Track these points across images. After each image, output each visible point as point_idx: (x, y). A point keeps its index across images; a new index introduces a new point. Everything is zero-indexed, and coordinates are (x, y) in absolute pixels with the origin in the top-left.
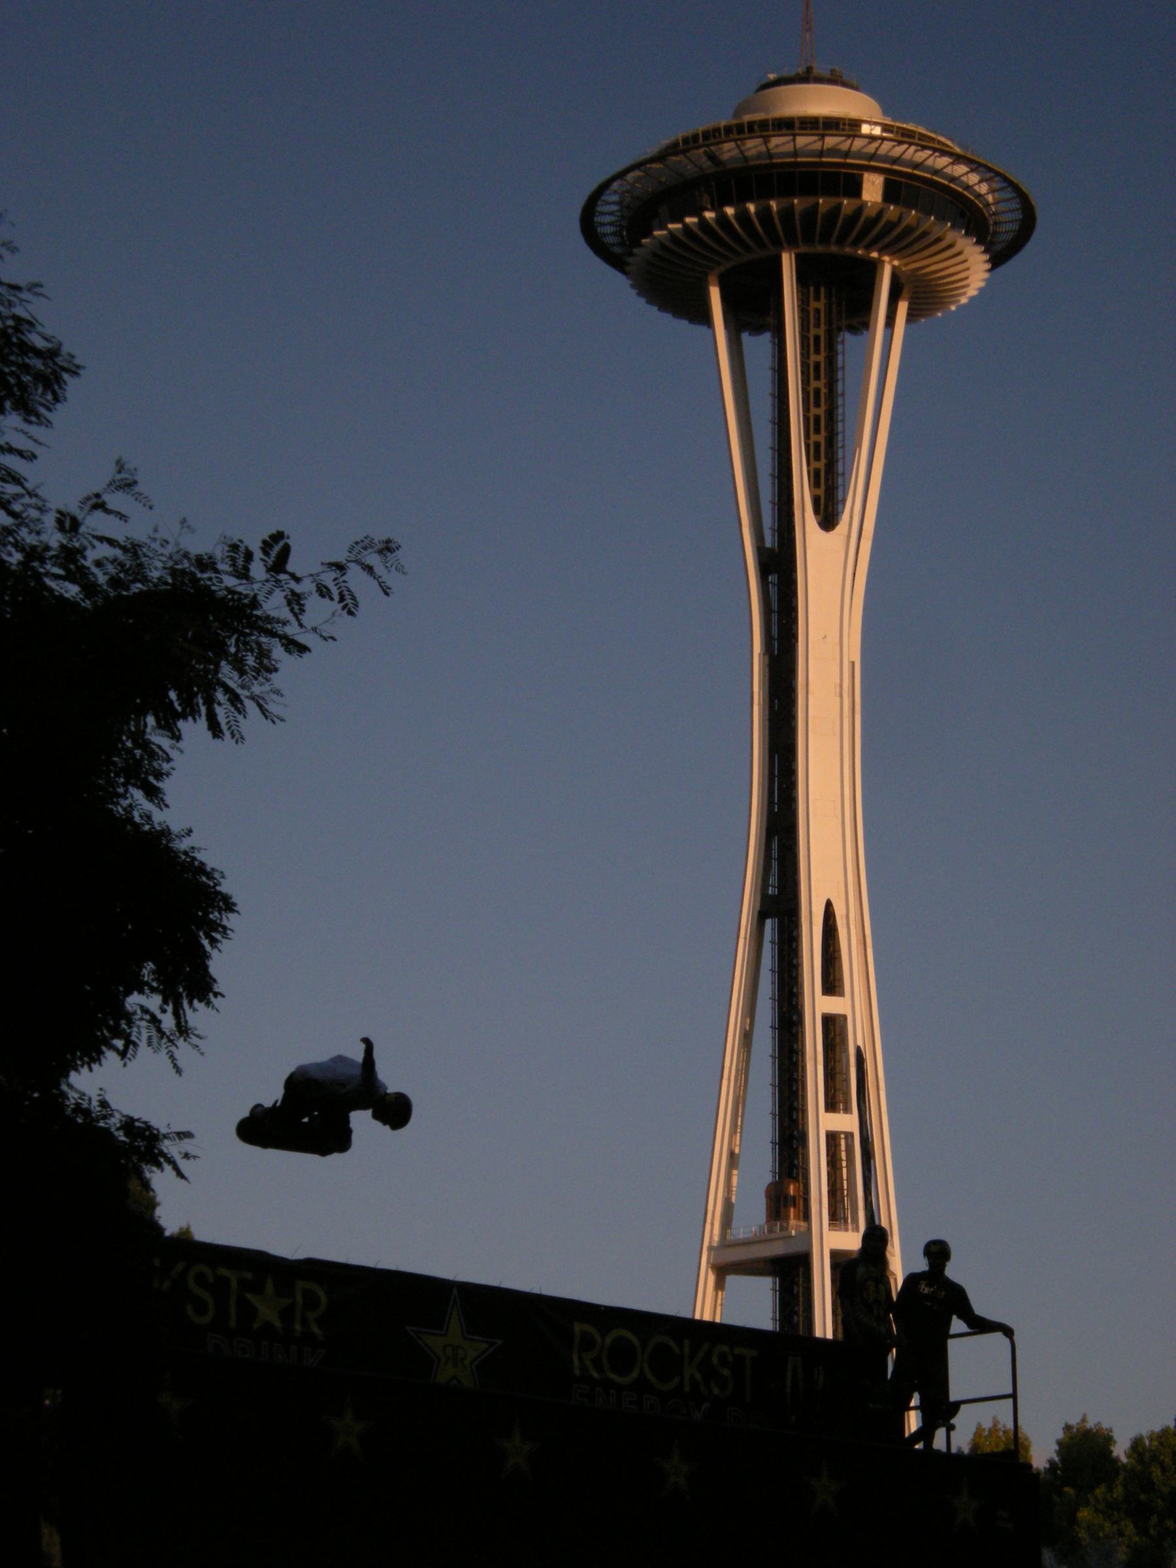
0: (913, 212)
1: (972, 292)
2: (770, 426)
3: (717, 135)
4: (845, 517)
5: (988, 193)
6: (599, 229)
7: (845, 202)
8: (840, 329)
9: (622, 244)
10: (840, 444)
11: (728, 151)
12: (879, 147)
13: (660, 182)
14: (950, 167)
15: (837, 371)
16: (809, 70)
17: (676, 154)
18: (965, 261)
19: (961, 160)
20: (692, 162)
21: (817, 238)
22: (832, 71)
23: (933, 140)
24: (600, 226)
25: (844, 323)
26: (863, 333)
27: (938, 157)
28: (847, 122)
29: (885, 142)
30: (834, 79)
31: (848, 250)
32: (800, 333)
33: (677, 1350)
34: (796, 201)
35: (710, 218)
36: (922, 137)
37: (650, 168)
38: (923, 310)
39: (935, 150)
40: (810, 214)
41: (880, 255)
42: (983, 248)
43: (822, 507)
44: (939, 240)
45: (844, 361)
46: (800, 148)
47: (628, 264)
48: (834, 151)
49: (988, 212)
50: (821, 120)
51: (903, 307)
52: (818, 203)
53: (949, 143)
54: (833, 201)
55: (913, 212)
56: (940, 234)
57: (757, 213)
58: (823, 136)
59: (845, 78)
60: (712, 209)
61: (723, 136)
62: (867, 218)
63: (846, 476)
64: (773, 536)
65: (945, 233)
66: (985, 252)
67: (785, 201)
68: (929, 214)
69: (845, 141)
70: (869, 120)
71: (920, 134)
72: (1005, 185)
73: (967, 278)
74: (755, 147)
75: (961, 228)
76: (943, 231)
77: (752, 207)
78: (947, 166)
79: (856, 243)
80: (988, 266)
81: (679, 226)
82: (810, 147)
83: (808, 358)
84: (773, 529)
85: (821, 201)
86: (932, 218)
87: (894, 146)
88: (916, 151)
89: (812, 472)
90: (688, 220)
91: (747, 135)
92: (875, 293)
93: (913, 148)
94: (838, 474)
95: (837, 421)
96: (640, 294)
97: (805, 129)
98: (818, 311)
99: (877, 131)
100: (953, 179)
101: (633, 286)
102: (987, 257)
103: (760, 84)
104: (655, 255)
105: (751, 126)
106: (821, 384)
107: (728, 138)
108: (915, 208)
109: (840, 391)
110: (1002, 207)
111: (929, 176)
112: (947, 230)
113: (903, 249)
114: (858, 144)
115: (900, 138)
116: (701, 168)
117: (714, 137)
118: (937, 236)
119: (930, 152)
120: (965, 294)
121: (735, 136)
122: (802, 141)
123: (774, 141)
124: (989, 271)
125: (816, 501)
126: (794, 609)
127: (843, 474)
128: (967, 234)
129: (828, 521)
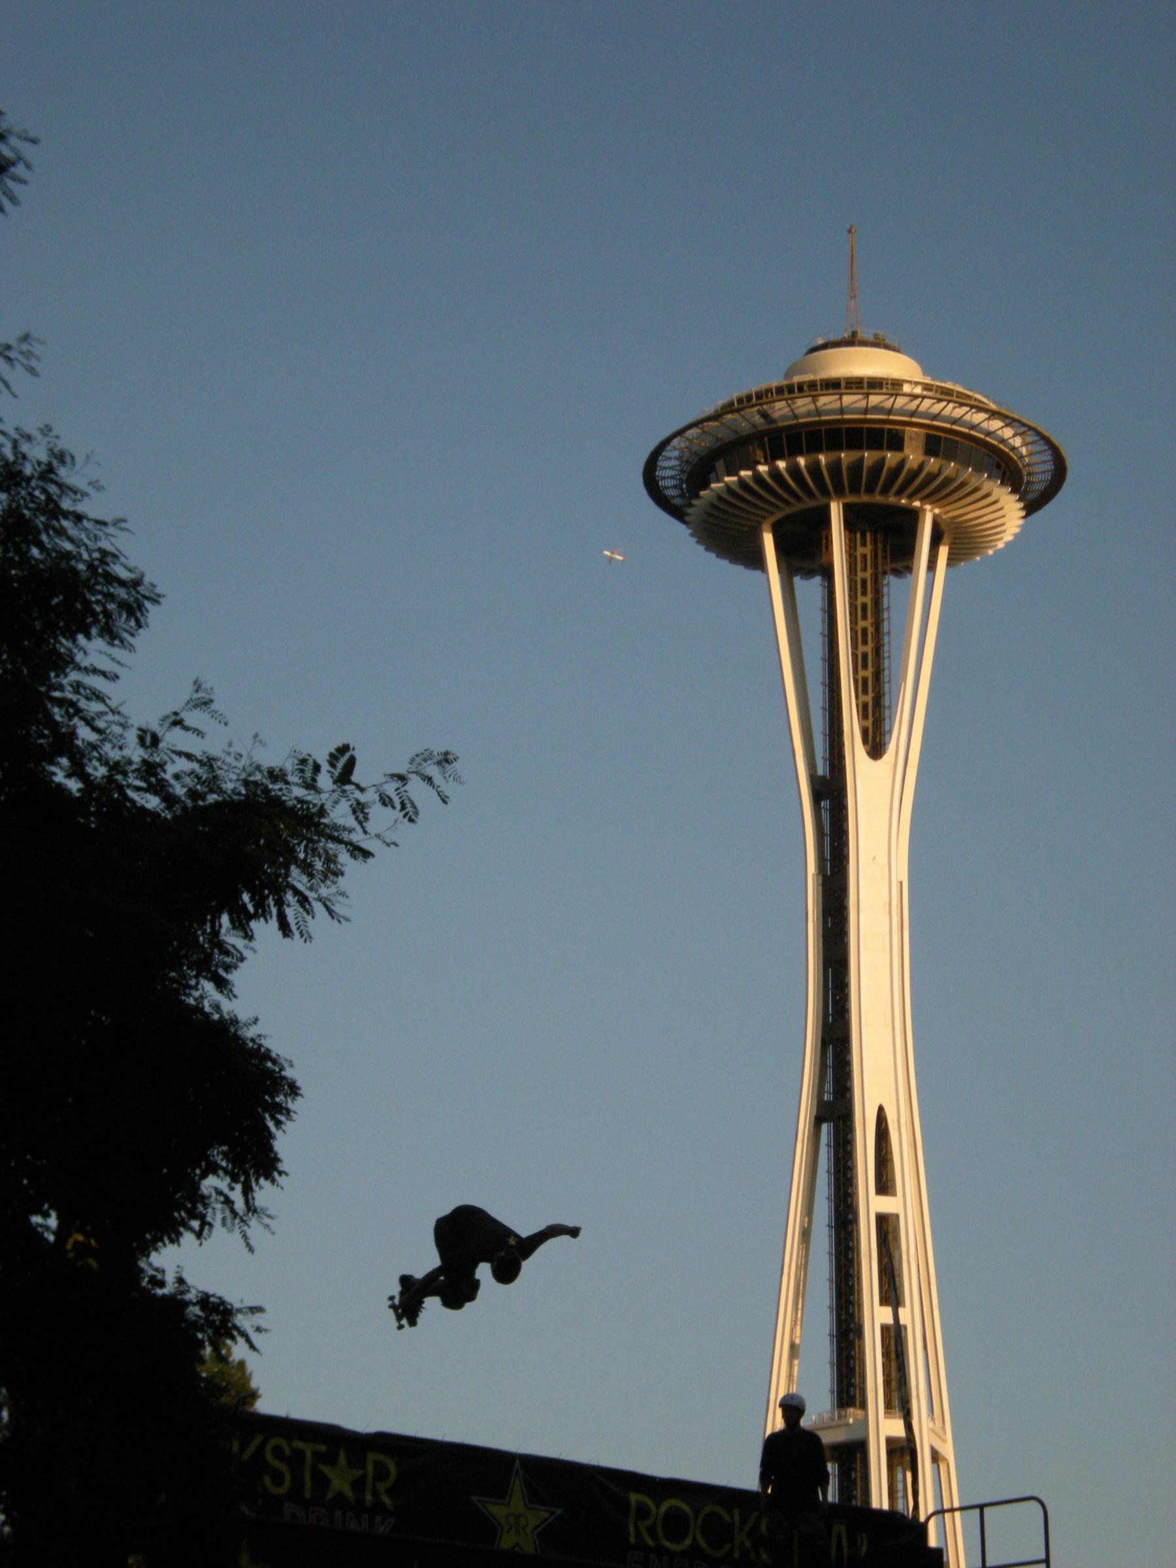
0: (952, 464)
1: (1008, 537)
3: (770, 395)
4: (891, 748)
5: (1021, 446)
6: (660, 484)
7: (889, 455)
8: (885, 573)
9: (682, 496)
10: (886, 679)
11: (779, 409)
12: (920, 404)
13: (717, 439)
14: (986, 422)
16: (854, 334)
17: (732, 412)
18: (1001, 509)
19: (996, 416)
20: (746, 420)
22: (876, 336)
23: (970, 397)
24: (661, 479)
25: (888, 567)
26: (906, 577)
27: (975, 413)
29: (925, 400)
30: (877, 343)
31: (892, 499)
32: (847, 576)
34: (843, 455)
35: (765, 472)
36: (960, 395)
37: (708, 426)
38: (964, 554)
39: (972, 407)
40: (857, 467)
42: (1018, 497)
43: (870, 738)
44: (976, 490)
45: (889, 602)
46: (846, 407)
47: (688, 514)
48: (877, 409)
49: (1023, 464)
50: (866, 381)
51: (944, 551)
52: (862, 459)
53: (985, 400)
55: (952, 464)
56: (977, 484)
57: (806, 466)
58: (867, 395)
59: (889, 342)
60: (766, 463)
61: (775, 395)
62: (909, 470)
63: (892, 708)
64: (825, 764)
65: (982, 484)
66: (1020, 500)
67: (833, 455)
69: (888, 399)
70: (910, 379)
71: (958, 392)
72: (1036, 438)
73: (1003, 524)
74: (804, 405)
76: (981, 481)
77: (802, 461)
78: (983, 421)
79: (899, 493)
80: (1023, 513)
81: (735, 479)
82: (855, 405)
83: (856, 599)
85: (866, 455)
86: (970, 469)
87: (934, 404)
88: (954, 408)
90: (743, 473)
91: (797, 394)
93: (951, 405)
94: (884, 707)
95: (884, 658)
97: (851, 388)
98: (864, 556)
99: (918, 390)
100: (989, 434)
101: (691, 535)
102: (1021, 505)
103: (808, 348)
104: (712, 506)
105: (801, 387)
106: (868, 624)
107: (779, 397)
109: (886, 630)
111: (966, 431)
112: (984, 481)
114: (901, 402)
115: (939, 396)
116: (754, 426)
118: (974, 486)
119: (967, 409)
120: (1001, 539)
121: (786, 396)
122: (848, 400)
123: (823, 400)
126: (846, 833)
127: (890, 707)
129: (876, 750)
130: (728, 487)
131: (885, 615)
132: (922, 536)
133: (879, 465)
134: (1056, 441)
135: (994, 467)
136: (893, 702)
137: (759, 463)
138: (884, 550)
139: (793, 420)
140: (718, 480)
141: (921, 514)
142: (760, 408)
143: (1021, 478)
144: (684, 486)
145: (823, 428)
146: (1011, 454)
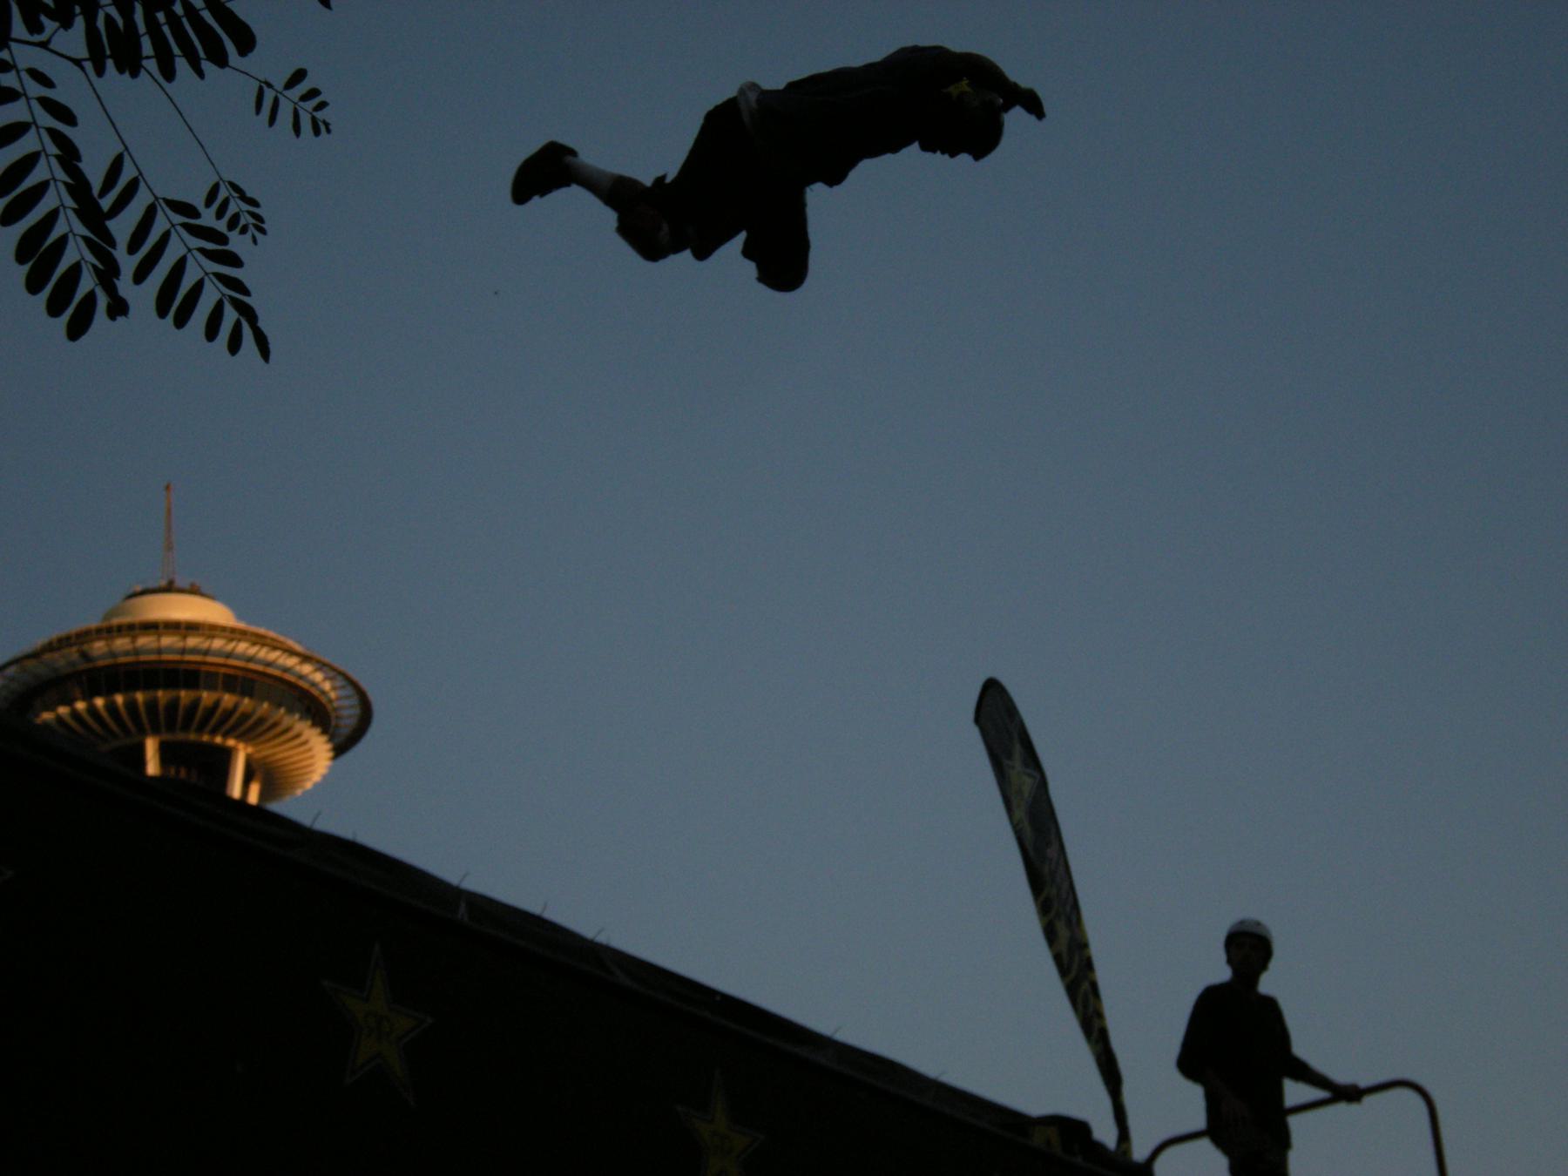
1: (316, 777)
11: (99, 647)
16: (171, 583)
22: (192, 585)
30: (194, 591)
31: (206, 738)
36: (273, 640)
40: (173, 705)
48: (195, 651)
58: (185, 637)
60: (84, 699)
62: (225, 711)
67: (150, 694)
68: (280, 706)
72: (344, 683)
77: (119, 699)
79: (214, 732)
88: (268, 653)
92: (231, 773)
100: (301, 677)
110: (346, 703)
113: (261, 735)
121: (105, 635)
122: (167, 641)
132: (234, 775)
133: (195, 704)
134: (364, 685)
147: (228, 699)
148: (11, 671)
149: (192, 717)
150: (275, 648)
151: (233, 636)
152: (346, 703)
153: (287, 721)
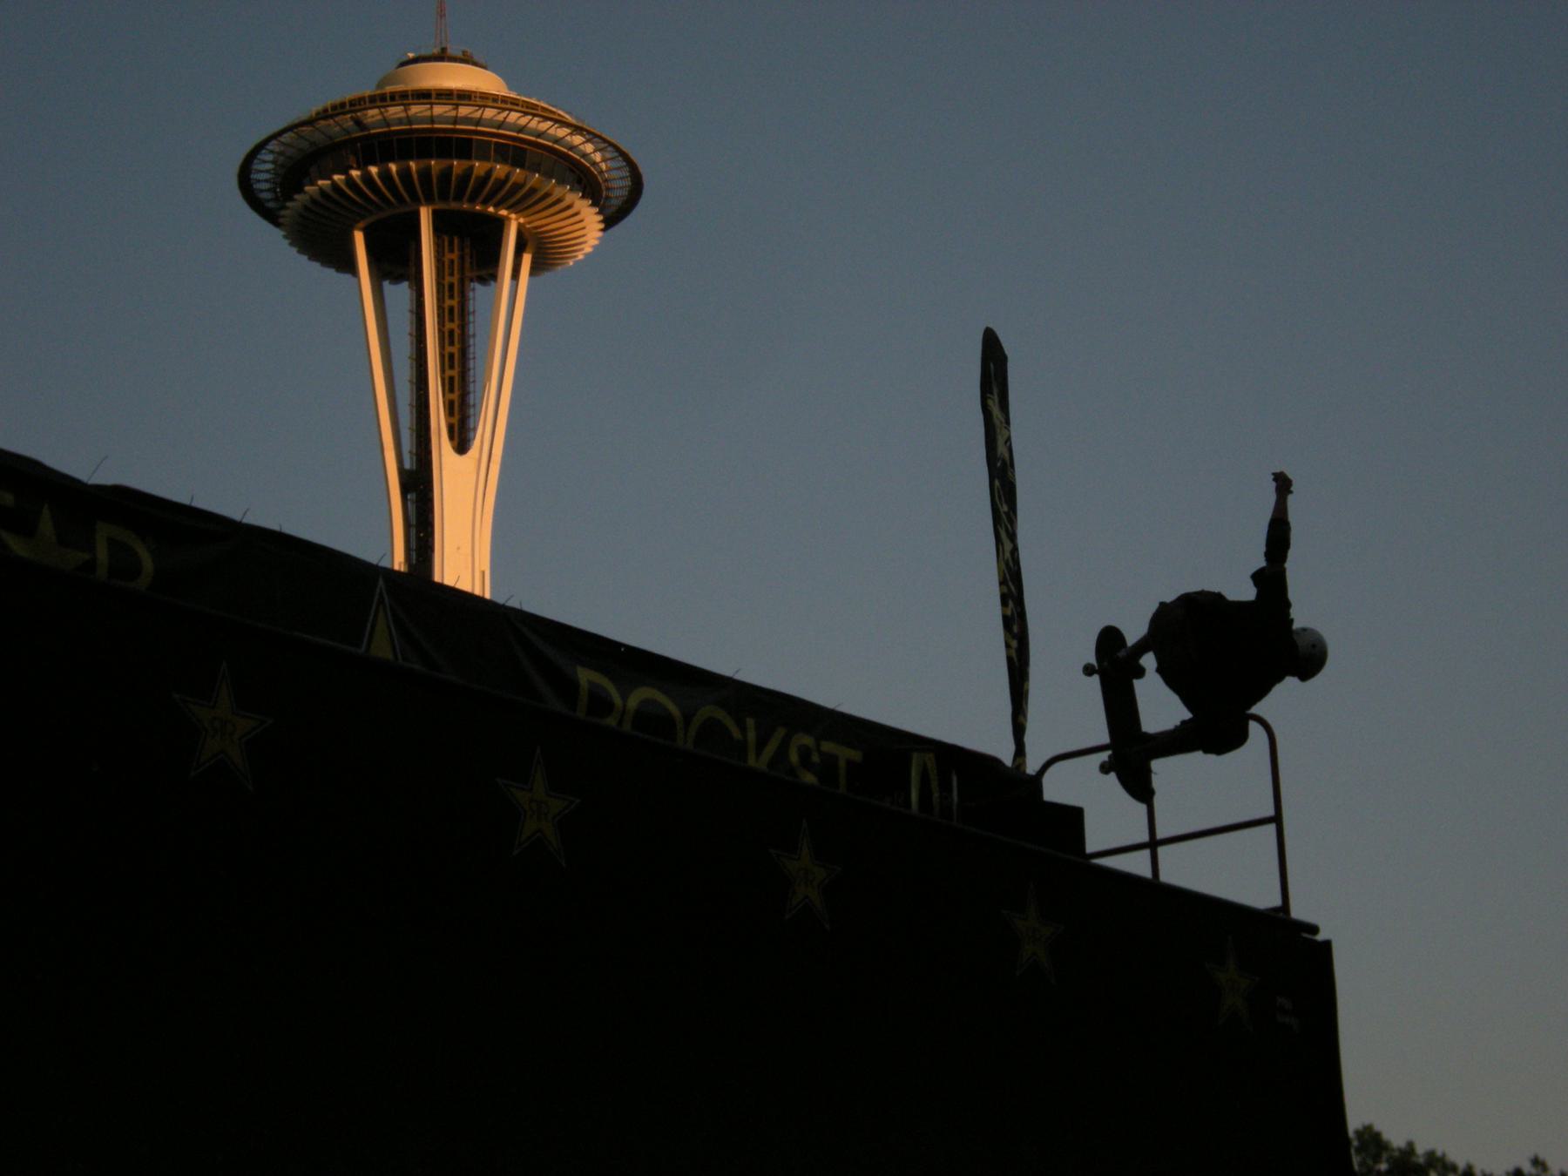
0: (537, 175)
1: (588, 249)
2: (409, 361)
3: (362, 103)
4: (476, 443)
5: (601, 162)
6: (254, 186)
7: (477, 164)
8: (472, 280)
9: (276, 199)
15: (469, 314)
16: (444, 50)
17: (325, 118)
18: (582, 221)
20: (340, 126)
21: (452, 195)
22: (464, 53)
26: (489, 285)
28: (478, 95)
30: (466, 59)
33: (736, 734)
34: (433, 162)
35: (357, 176)
37: (303, 131)
39: (556, 121)
40: (446, 174)
41: (509, 214)
43: (456, 434)
44: (559, 201)
46: (440, 116)
47: (283, 216)
48: (467, 120)
50: (455, 93)
51: (527, 259)
52: (451, 167)
53: (567, 116)
54: (466, 163)
55: (537, 175)
56: (561, 195)
57: (397, 171)
58: (457, 106)
59: (476, 59)
62: (496, 179)
63: (478, 406)
64: (411, 458)
65: (564, 195)
66: (599, 213)
67: (423, 163)
68: (551, 177)
69: (477, 110)
72: (616, 154)
73: (584, 236)
74: (396, 113)
75: (578, 190)
77: (393, 167)
78: (566, 136)
79: (485, 202)
80: (602, 226)
81: (328, 182)
82: (448, 114)
83: (444, 302)
84: (411, 452)
85: (455, 163)
87: (520, 117)
88: (539, 122)
89: (447, 402)
90: (336, 177)
91: (389, 103)
92: (503, 245)
93: (536, 119)
94: (469, 406)
95: (469, 359)
96: (291, 244)
97: (442, 99)
98: (452, 261)
100: (572, 148)
102: (600, 218)
103: (398, 63)
105: (393, 96)
106: (455, 326)
107: (373, 105)
108: (539, 173)
109: (471, 332)
110: (615, 174)
111: (550, 144)
113: (529, 207)
116: (347, 132)
117: (360, 104)
119: (550, 123)
120: (582, 249)
121: (379, 104)
122: (438, 110)
124: (603, 230)
125: (451, 428)
126: (431, 525)
127: (474, 405)
128: (583, 197)
129: (462, 447)
130: (322, 191)
131: (471, 318)
133: (469, 171)
135: (576, 185)
136: (477, 401)
137: (352, 168)
138: (471, 257)
139: (382, 128)
140: (313, 183)
141: (506, 222)
142: (354, 115)
143: (600, 191)
144: (278, 190)
145: (416, 135)
146: (592, 169)
147: (500, 169)
148: (286, 138)
149: (465, 186)
150: (547, 119)
151: (503, 106)
152: (615, 174)
153: (558, 192)
